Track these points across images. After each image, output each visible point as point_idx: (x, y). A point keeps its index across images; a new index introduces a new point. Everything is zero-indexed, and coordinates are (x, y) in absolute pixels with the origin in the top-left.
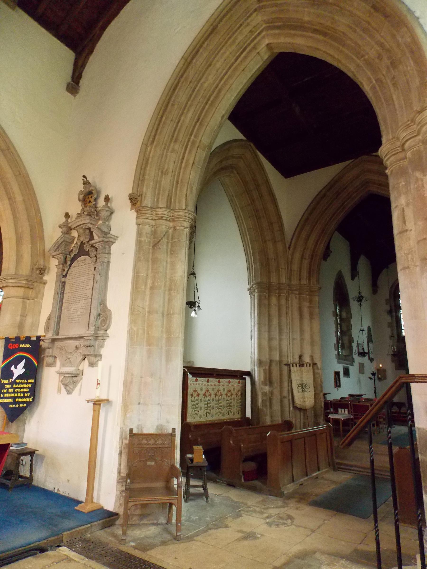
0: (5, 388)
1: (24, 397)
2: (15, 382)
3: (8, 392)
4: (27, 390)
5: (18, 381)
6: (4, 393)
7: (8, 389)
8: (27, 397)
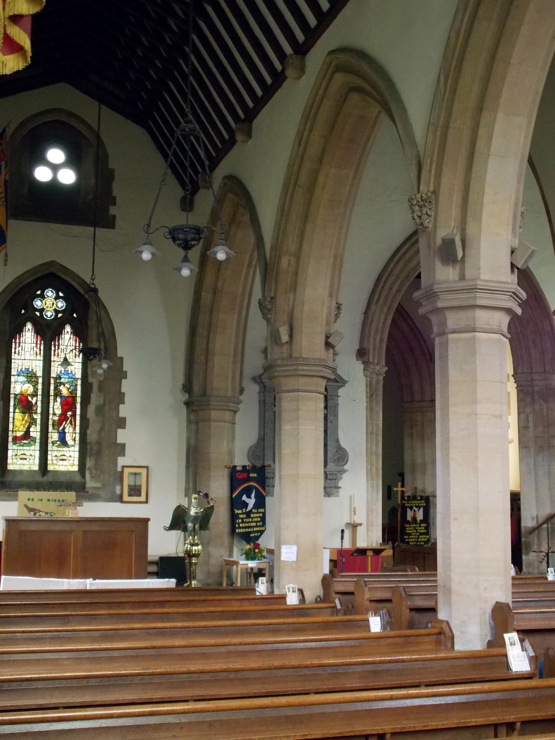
0: (239, 518)
1: (257, 526)
2: (251, 511)
3: (243, 522)
4: (259, 519)
5: (253, 510)
6: (239, 524)
7: (243, 519)
8: (260, 526)
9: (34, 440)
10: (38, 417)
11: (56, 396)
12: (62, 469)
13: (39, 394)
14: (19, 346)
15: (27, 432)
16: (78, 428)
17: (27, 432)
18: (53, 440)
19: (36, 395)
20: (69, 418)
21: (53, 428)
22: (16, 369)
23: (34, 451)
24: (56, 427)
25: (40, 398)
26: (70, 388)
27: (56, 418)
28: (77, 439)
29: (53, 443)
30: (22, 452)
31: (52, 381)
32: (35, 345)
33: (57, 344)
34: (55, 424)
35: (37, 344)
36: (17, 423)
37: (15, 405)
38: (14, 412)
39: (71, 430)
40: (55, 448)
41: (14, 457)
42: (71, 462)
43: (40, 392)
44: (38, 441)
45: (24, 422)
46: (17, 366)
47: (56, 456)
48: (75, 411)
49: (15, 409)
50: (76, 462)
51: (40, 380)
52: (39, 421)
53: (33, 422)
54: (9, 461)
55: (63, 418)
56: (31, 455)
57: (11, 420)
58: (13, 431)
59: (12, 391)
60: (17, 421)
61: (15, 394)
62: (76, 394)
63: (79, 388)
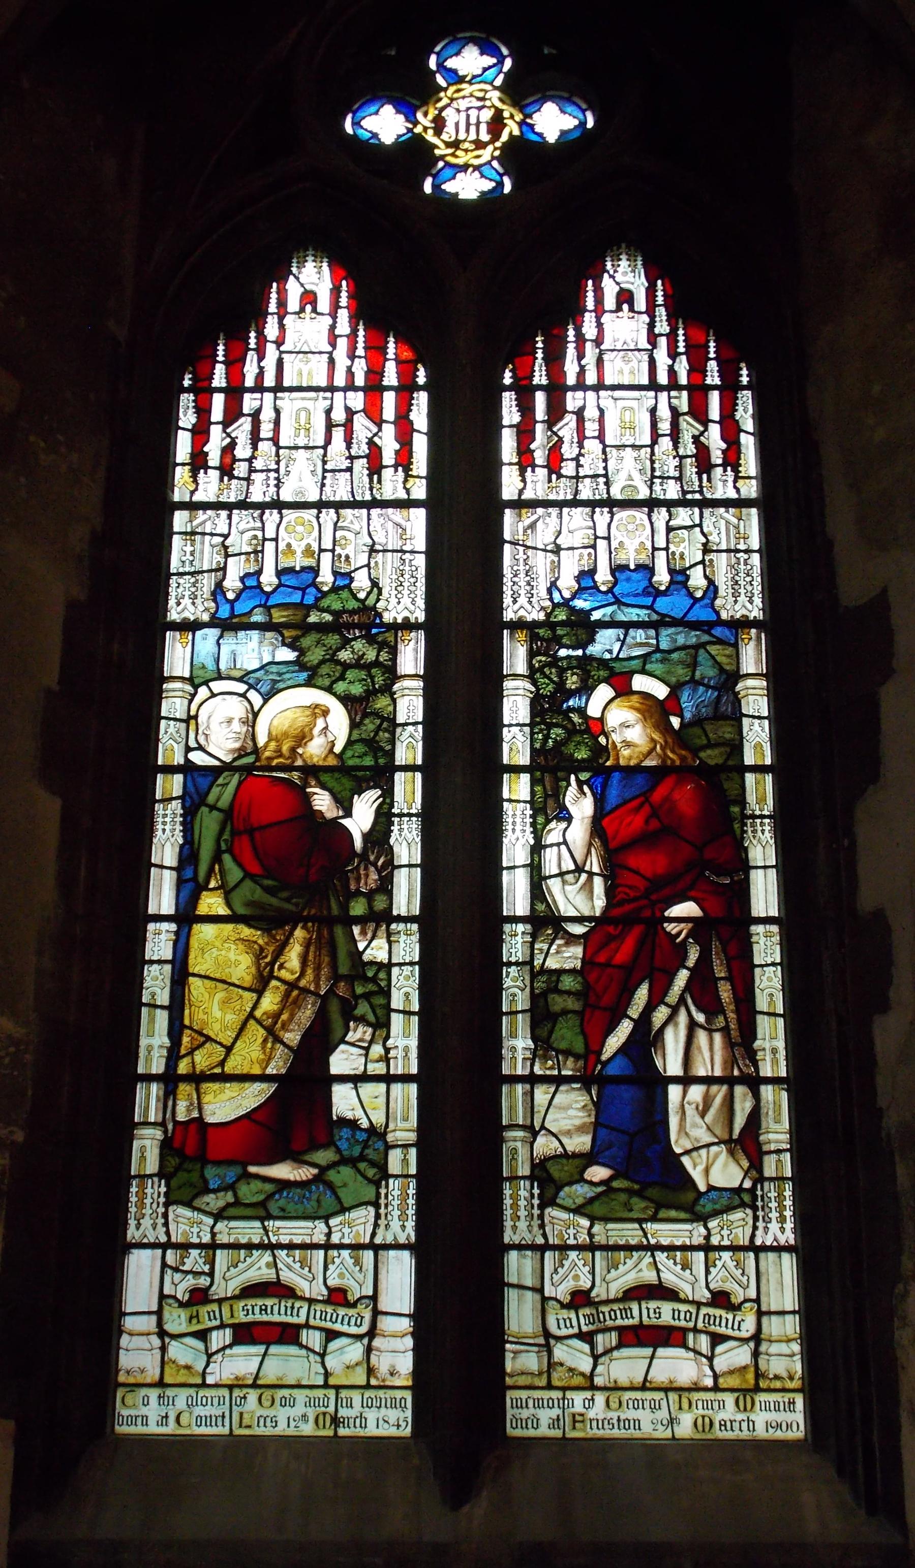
9: (367, 1148)
10: (397, 952)
11: (549, 768)
12: (649, 1422)
13: (402, 756)
14: (233, 414)
15: (301, 1092)
16: (772, 1040)
17: (301, 1092)
18: (544, 1145)
19: (382, 775)
20: (681, 952)
21: (543, 1045)
22: (207, 583)
23: (371, 1260)
24: (567, 1034)
25: (408, 791)
26: (671, 705)
27: (566, 957)
28: (777, 1132)
29: (548, 1179)
30: (259, 1268)
31: (516, 656)
32: (357, 400)
33: (540, 377)
34: (558, 1003)
35: (374, 388)
36: (213, 1011)
37: (188, 855)
38: (186, 917)
39: (711, 1057)
40: (564, 1224)
41: (177, 1321)
42: (736, 1356)
43: (409, 748)
45: (269, 1002)
46: (209, 558)
47: (580, 1299)
48: (741, 892)
49: (190, 887)
50: (785, 1359)
51: (411, 656)
52: (405, 989)
53: (355, 995)
54: (136, 1355)
55: (626, 950)
56: (337, 1297)
57: (156, 984)
58: (170, 1080)
59: (170, 747)
60: (212, 982)
61: (188, 768)
62: (736, 747)
63: (755, 700)
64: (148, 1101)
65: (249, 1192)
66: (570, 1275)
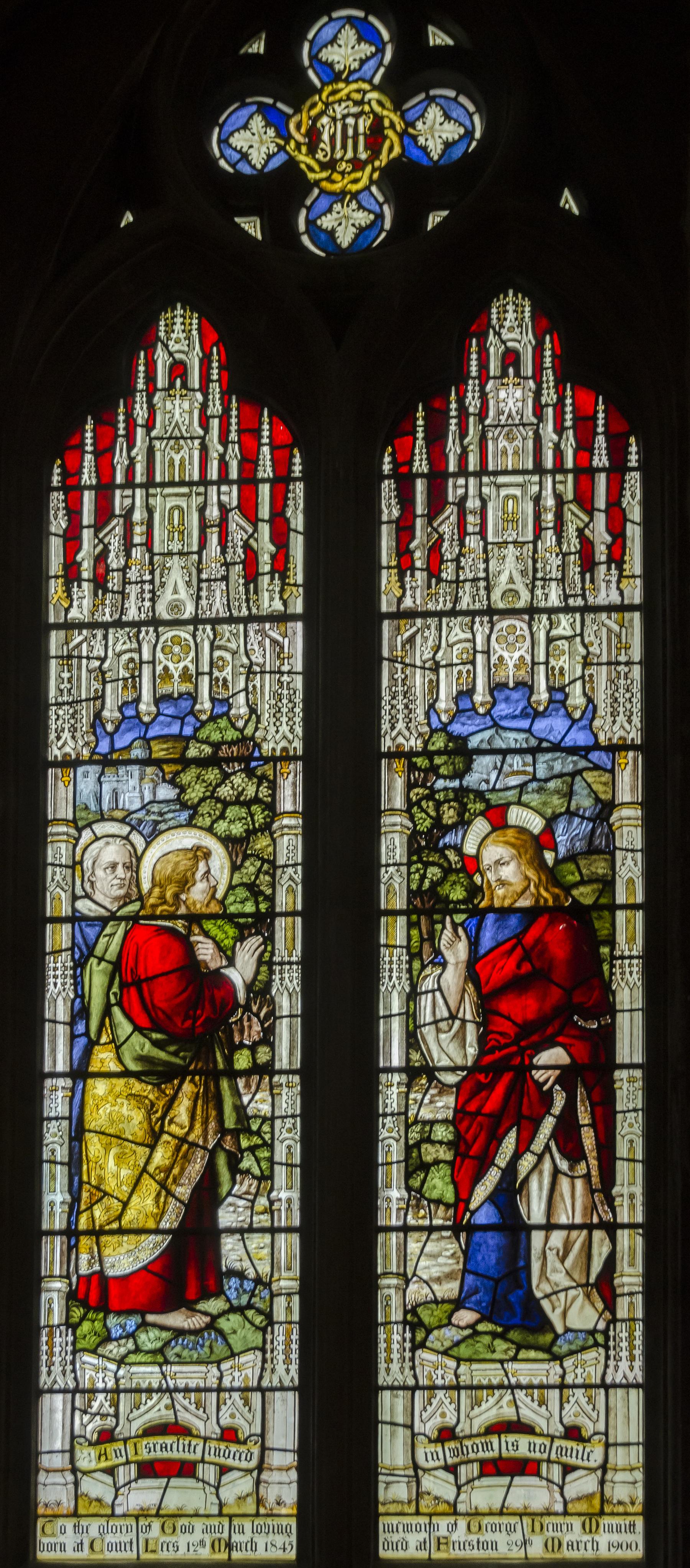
16: (630, 1183)
21: (416, 1196)
26: (545, 840)
28: (630, 1277)
34: (430, 1153)
42: (583, 1484)
44: (287, 1309)
45: (161, 1156)
47: (446, 1434)
50: (628, 1487)
52: (288, 1142)
55: (495, 1103)
58: (71, 1233)
62: (608, 884)
63: (630, 833)
64: (53, 1252)
65: (149, 1339)
66: (437, 1413)
